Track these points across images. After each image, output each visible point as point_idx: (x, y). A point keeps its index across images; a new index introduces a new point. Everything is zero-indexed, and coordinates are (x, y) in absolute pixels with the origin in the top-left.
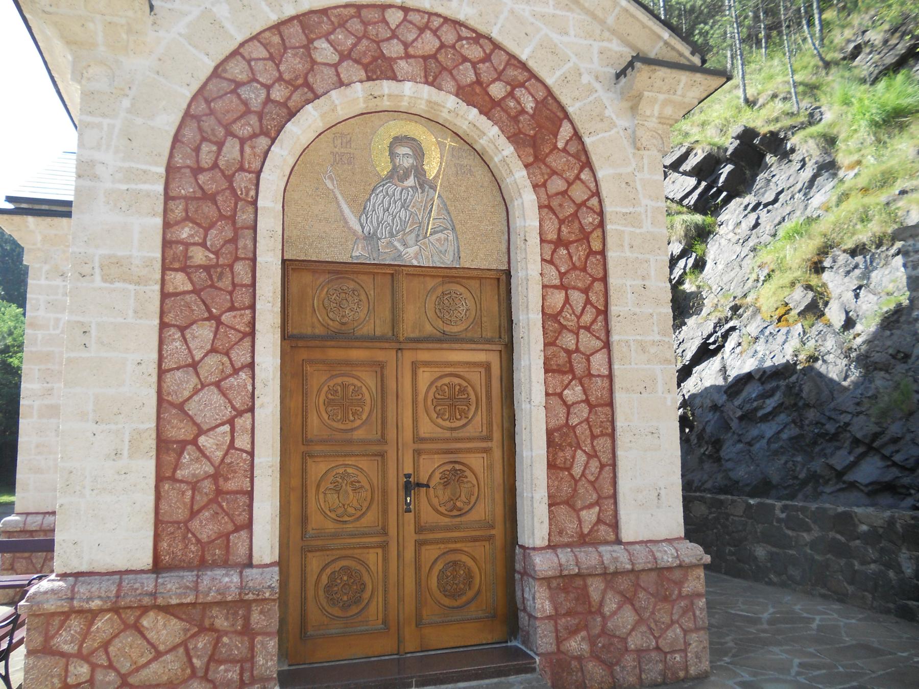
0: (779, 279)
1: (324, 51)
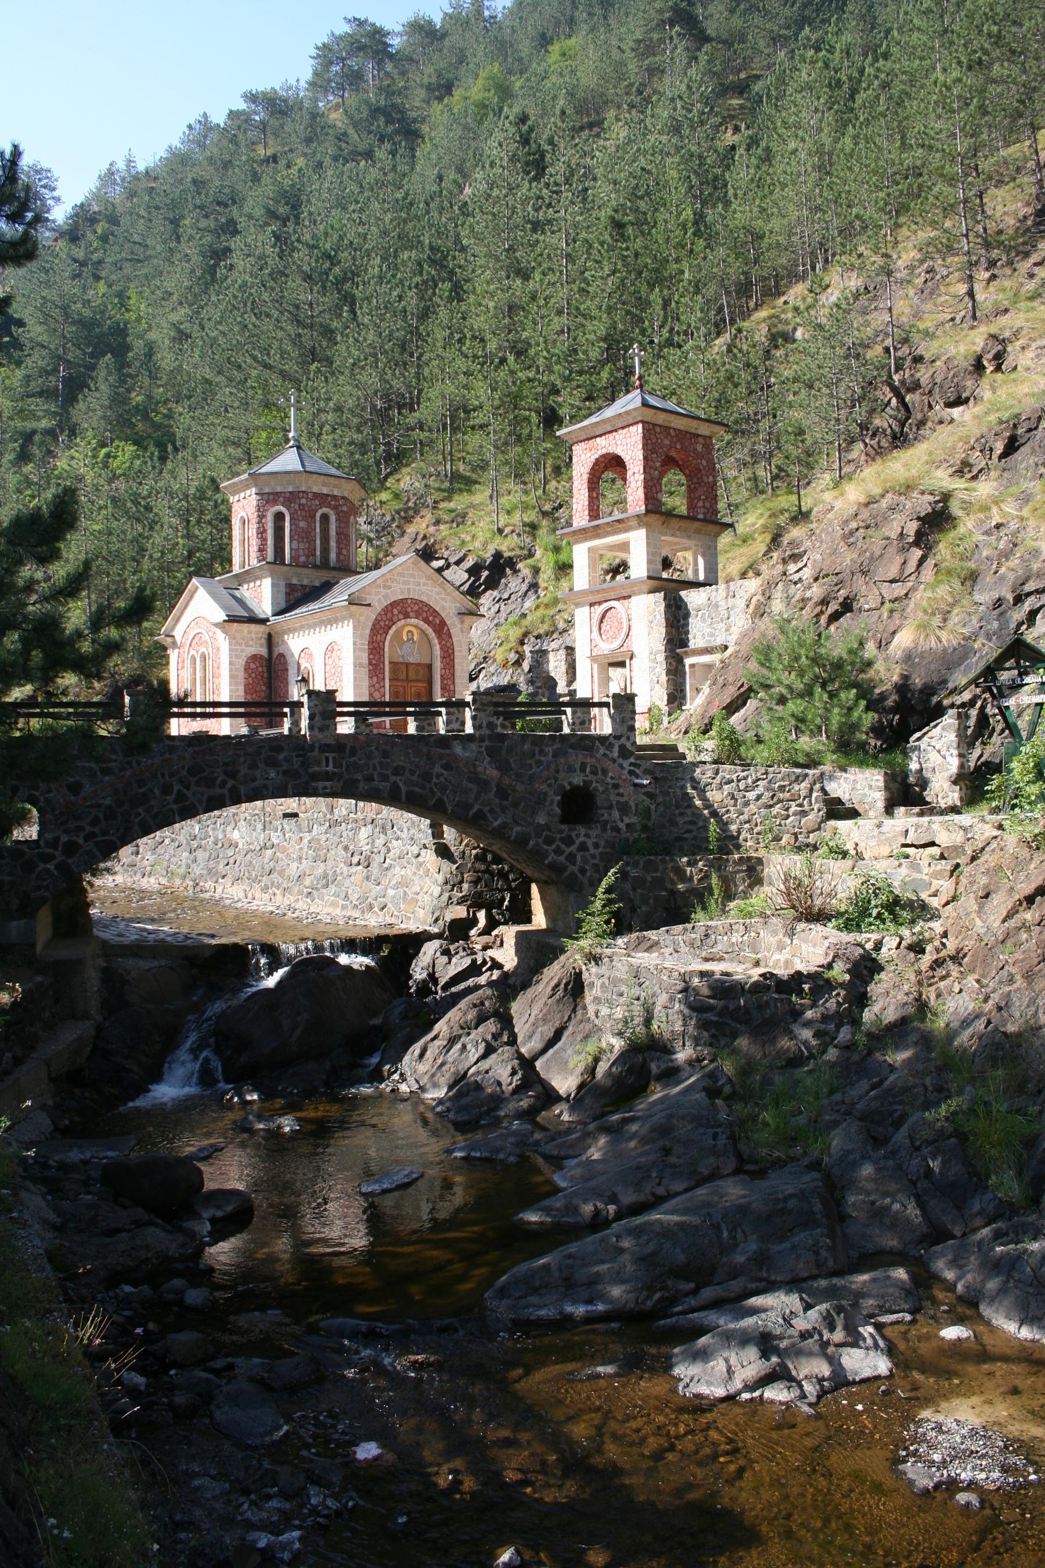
0: (506, 647)
1: (396, 612)
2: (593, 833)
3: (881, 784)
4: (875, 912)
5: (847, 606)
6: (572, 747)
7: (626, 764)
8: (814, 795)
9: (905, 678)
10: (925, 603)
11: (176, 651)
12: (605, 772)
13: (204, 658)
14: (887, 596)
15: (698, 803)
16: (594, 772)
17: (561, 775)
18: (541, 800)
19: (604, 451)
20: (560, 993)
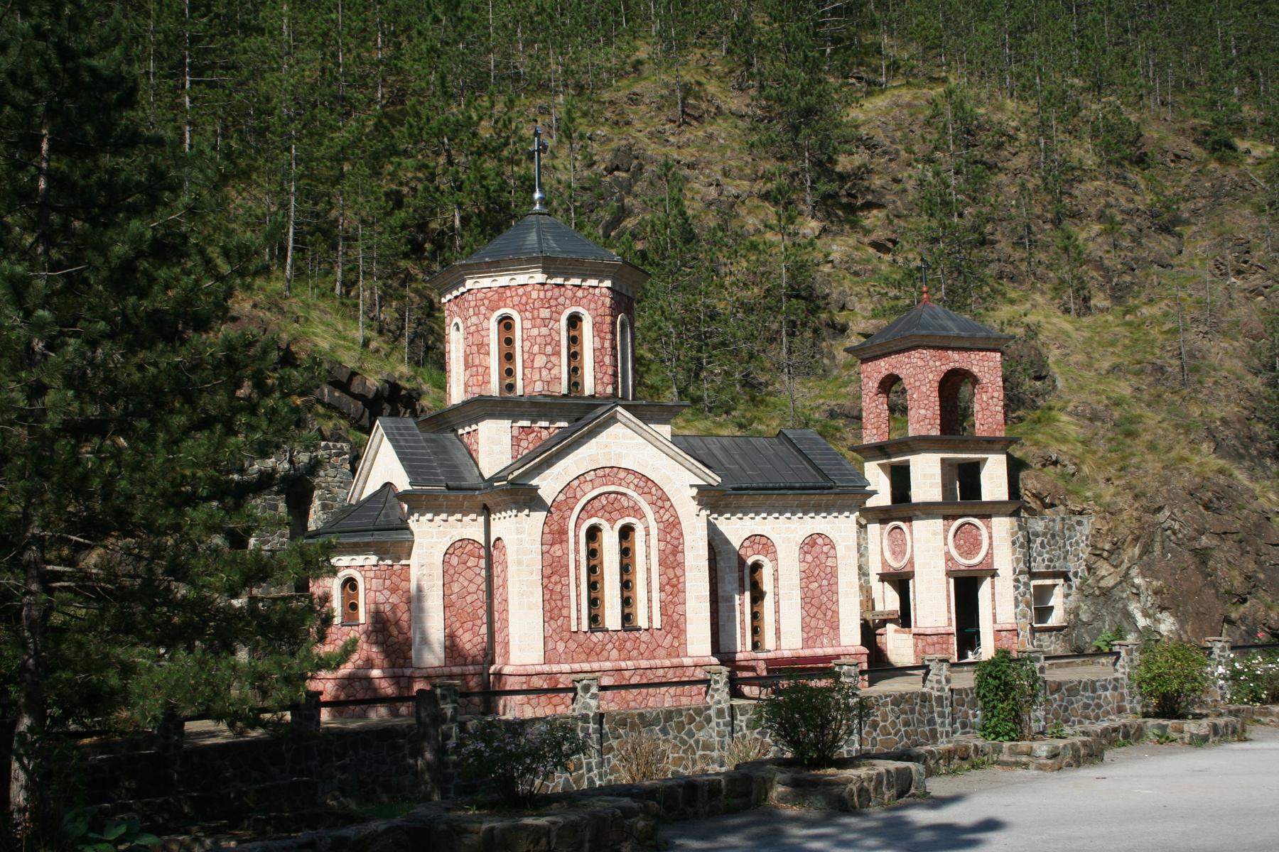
11: (540, 516)
13: (626, 532)
19: (957, 365)
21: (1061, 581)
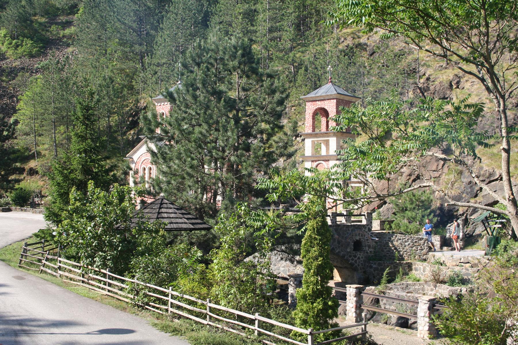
2: (361, 254)
3: (439, 240)
4: (457, 281)
5: (418, 177)
6: (356, 228)
7: (370, 233)
8: (425, 244)
9: (442, 205)
10: (446, 180)
12: (365, 236)
14: (433, 176)
15: (391, 245)
16: (362, 236)
17: (354, 237)
18: (348, 244)
19: (320, 106)
20: (373, 302)
21: (362, 185)
